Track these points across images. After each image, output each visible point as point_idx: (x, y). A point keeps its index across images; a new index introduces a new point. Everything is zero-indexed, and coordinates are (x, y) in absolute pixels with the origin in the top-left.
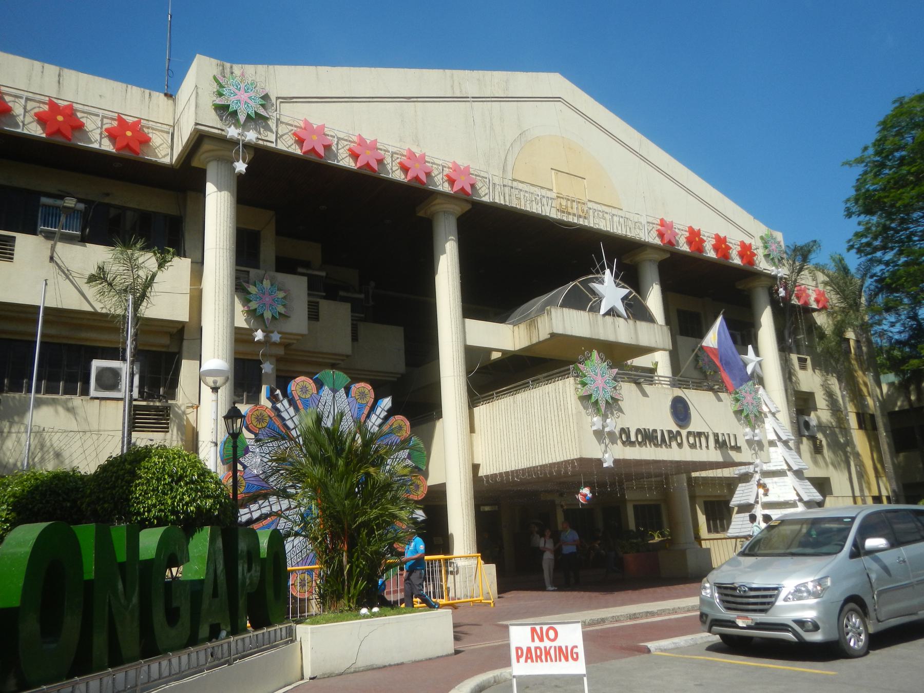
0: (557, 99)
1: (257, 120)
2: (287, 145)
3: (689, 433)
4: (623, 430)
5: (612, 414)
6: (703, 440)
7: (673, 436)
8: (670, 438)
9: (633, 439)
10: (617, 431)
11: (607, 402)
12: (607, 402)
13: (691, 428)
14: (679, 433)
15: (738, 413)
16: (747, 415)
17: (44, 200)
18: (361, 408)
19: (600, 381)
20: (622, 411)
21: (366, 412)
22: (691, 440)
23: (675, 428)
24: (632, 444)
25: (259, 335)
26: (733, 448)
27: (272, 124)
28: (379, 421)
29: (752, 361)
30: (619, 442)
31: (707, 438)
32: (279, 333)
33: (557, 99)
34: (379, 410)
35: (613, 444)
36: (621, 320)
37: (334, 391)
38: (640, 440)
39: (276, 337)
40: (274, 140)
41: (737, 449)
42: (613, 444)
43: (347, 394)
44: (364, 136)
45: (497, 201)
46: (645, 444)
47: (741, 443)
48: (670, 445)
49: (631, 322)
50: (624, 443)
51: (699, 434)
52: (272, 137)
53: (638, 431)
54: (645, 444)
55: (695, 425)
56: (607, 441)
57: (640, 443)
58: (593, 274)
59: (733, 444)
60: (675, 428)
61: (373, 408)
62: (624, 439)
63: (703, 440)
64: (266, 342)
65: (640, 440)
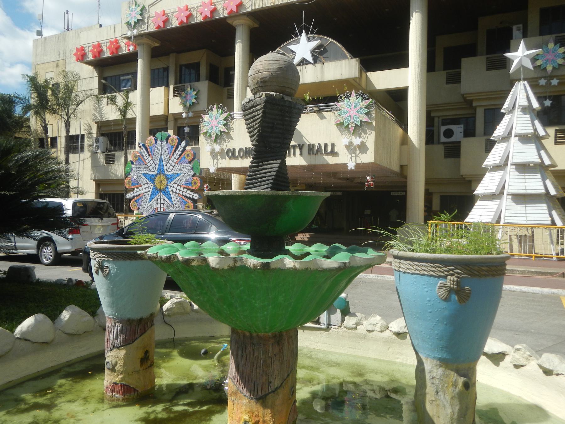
1: (139, 22)
2: (152, 28)
4: (229, 150)
5: (225, 141)
6: (298, 151)
9: (237, 154)
10: (226, 151)
11: (217, 134)
12: (217, 134)
15: (340, 125)
16: (348, 126)
17: (122, 78)
18: (172, 148)
19: (214, 123)
20: (232, 139)
21: (174, 149)
24: (236, 158)
25: (184, 115)
26: (327, 154)
27: (146, 21)
28: (180, 153)
29: (517, 57)
30: (227, 157)
32: (192, 112)
34: (180, 147)
35: (222, 159)
36: (311, 65)
37: (161, 141)
39: (191, 115)
40: (146, 28)
41: (333, 153)
42: (222, 159)
43: (167, 142)
44: (179, 6)
45: (257, 7)
46: (246, 157)
47: (340, 148)
49: (318, 65)
50: (230, 158)
52: (145, 27)
53: (240, 150)
54: (246, 157)
56: (219, 157)
57: (242, 157)
58: (293, 38)
59: (329, 150)
61: (177, 147)
64: (187, 117)
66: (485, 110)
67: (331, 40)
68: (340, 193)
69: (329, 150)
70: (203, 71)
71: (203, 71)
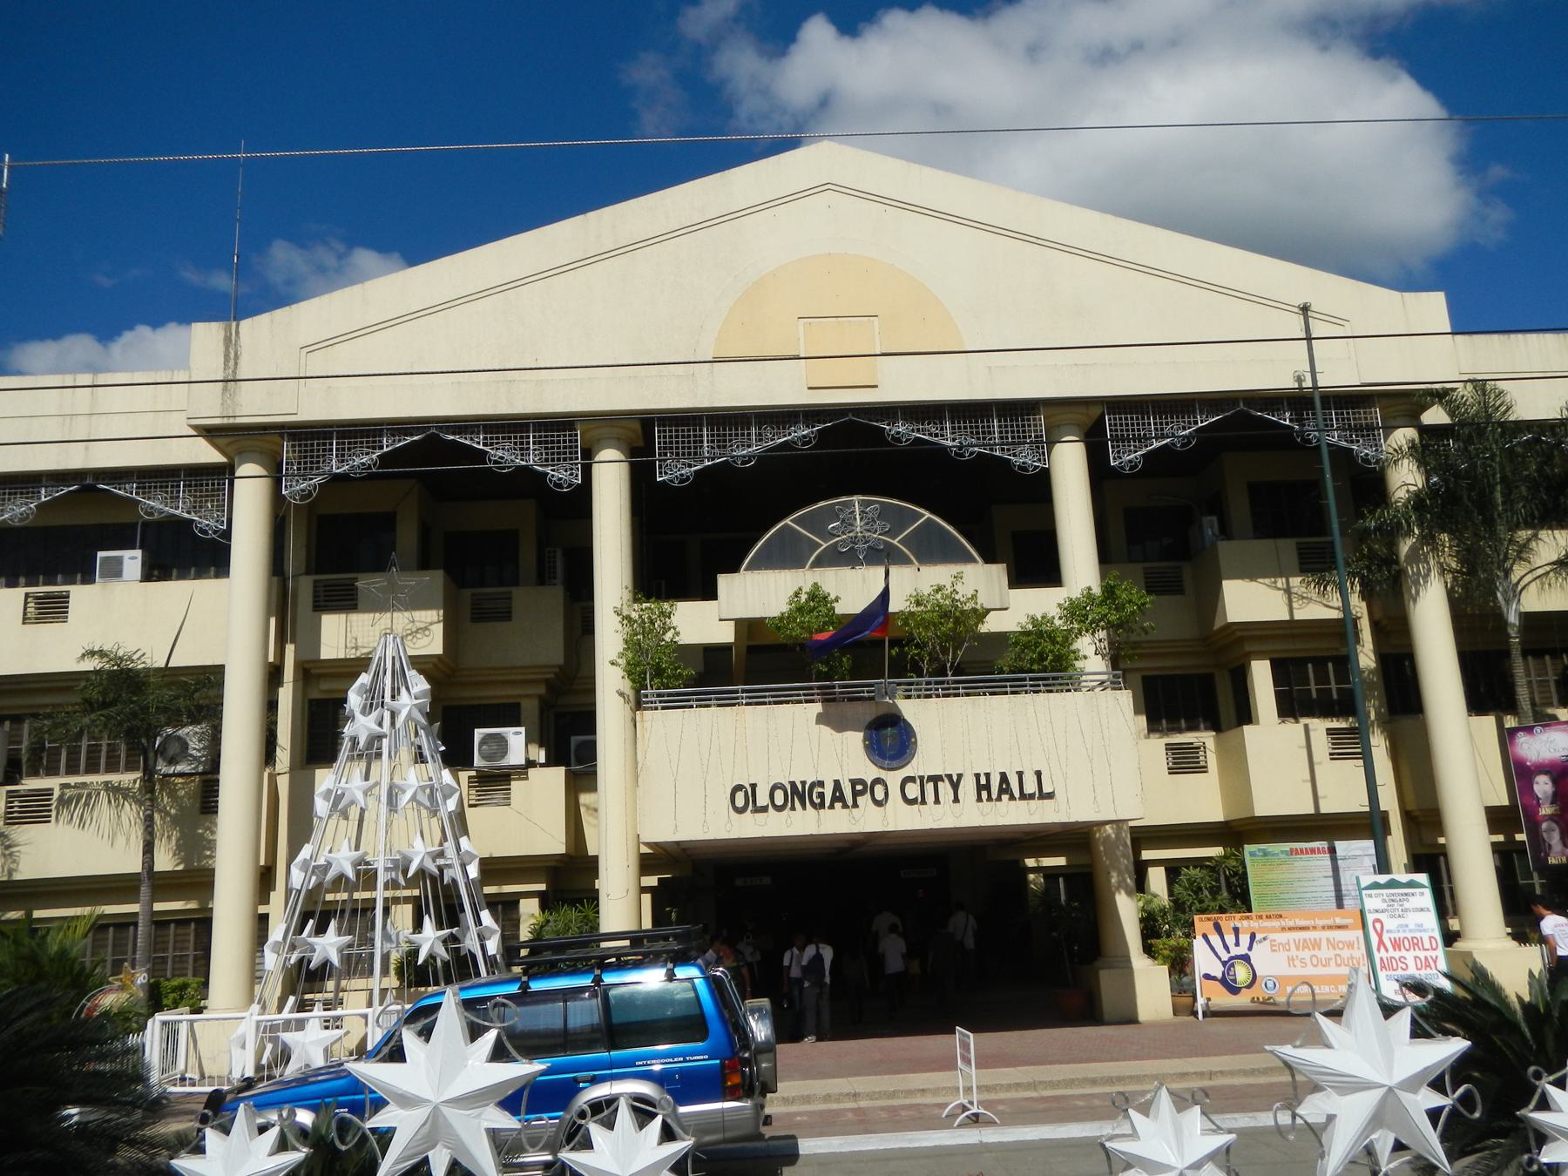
0: (824, 187)
3: (911, 779)
6: (945, 787)
7: (861, 788)
8: (855, 794)
9: (763, 799)
13: (918, 766)
14: (877, 781)
22: (913, 791)
23: (870, 772)
31: (955, 786)
33: (824, 187)
38: (779, 800)
48: (855, 805)
51: (935, 779)
55: (922, 763)
57: (780, 809)
60: (870, 772)
62: (740, 802)
63: (945, 787)
65: (779, 800)
66: (1144, 679)
67: (928, 515)
68: (767, 880)
69: (1031, 787)
70: (407, 536)
71: (407, 536)
